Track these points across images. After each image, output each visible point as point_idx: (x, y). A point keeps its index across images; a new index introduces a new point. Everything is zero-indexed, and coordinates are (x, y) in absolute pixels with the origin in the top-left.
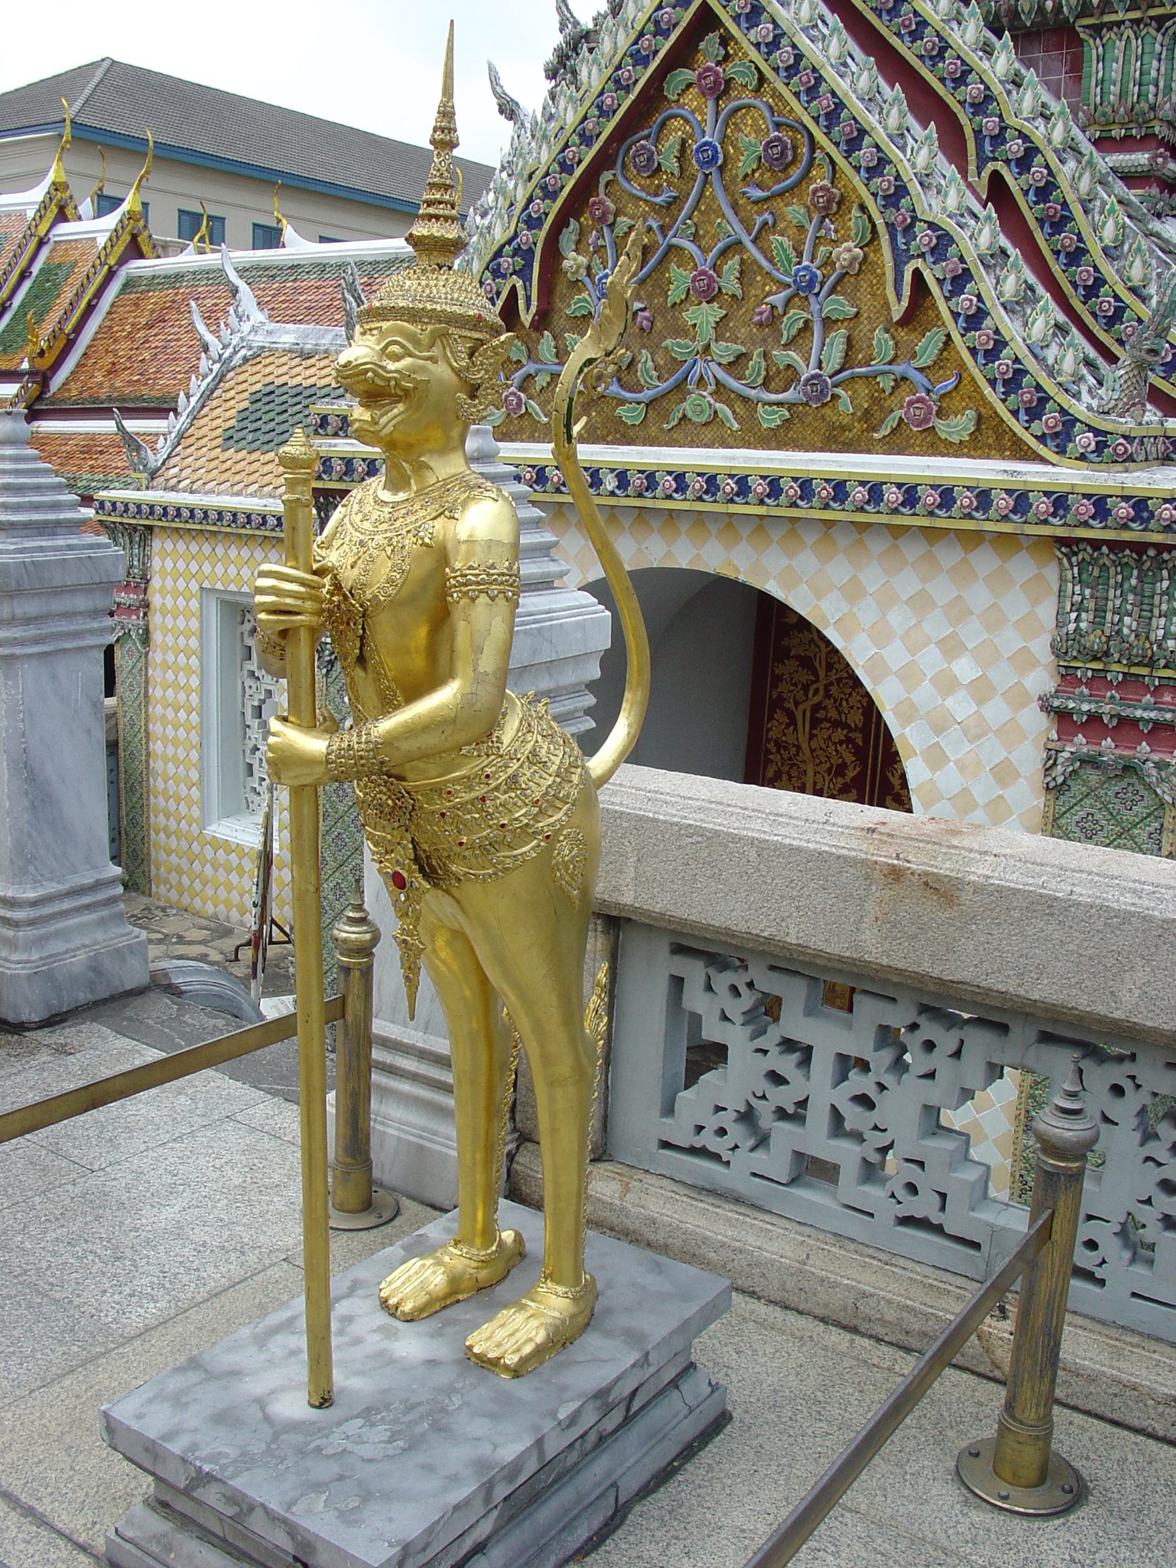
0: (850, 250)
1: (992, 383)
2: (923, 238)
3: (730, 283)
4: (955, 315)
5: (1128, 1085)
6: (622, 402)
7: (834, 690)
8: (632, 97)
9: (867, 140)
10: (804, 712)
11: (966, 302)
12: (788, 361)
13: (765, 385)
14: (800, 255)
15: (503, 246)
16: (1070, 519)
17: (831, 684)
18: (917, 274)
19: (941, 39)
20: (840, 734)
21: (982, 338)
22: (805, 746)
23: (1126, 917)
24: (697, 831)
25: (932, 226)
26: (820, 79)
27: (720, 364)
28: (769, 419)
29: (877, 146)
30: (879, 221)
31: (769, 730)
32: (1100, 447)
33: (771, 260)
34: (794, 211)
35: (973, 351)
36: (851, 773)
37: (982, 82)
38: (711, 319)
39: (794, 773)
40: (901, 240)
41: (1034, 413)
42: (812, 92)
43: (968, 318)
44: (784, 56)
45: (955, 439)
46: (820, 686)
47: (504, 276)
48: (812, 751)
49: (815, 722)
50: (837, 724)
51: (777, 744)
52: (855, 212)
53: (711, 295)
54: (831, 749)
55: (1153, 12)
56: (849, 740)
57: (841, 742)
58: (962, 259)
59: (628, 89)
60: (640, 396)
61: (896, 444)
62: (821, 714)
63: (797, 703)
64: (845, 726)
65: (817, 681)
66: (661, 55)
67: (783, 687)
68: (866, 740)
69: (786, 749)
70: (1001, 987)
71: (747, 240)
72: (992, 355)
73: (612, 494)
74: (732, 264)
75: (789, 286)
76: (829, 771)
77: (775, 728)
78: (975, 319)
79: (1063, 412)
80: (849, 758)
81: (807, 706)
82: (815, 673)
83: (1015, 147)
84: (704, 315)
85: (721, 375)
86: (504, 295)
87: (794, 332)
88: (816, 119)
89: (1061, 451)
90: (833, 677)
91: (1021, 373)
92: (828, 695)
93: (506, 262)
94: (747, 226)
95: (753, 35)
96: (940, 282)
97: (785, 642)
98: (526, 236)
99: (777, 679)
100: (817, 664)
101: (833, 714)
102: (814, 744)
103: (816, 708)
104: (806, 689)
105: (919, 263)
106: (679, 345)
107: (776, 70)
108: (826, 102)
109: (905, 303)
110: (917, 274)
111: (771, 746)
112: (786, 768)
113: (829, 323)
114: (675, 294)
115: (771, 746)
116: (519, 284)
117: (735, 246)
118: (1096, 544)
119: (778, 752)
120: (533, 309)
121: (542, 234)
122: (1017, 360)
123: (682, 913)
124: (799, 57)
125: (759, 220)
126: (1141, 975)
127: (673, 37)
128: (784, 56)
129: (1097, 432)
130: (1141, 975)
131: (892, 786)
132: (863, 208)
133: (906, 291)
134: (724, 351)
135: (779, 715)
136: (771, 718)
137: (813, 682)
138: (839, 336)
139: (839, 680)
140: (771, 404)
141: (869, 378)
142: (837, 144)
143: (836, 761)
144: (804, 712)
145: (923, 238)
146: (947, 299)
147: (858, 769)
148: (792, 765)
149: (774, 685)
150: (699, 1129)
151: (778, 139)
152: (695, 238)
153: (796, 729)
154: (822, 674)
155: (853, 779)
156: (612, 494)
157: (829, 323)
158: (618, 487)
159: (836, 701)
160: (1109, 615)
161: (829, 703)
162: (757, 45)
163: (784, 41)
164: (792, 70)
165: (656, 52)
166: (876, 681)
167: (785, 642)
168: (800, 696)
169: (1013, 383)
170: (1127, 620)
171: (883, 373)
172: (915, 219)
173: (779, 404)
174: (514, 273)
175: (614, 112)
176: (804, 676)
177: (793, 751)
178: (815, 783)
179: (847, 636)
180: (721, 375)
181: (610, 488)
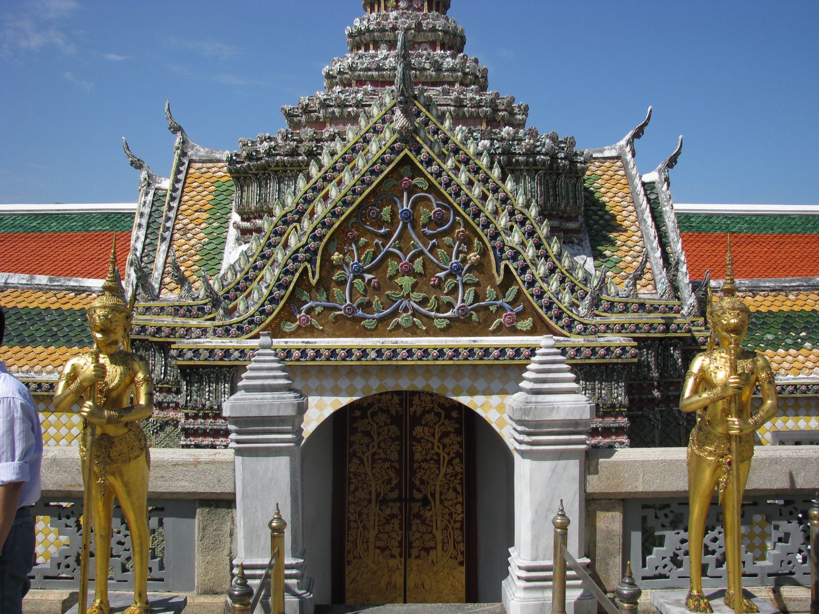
0: (475, 256)
1: (541, 307)
2: (508, 252)
3: (418, 265)
4: (524, 282)
5: (794, 510)
6: (365, 319)
7: (382, 445)
8: (370, 188)
9: (482, 214)
10: (368, 457)
11: (527, 276)
12: (448, 300)
13: (438, 311)
14: (451, 257)
15: (299, 249)
16: (582, 356)
17: (381, 442)
18: (506, 266)
19: (487, 175)
20: (387, 464)
21: (535, 290)
22: (369, 473)
23: (797, 459)
24: (665, 461)
25: (512, 248)
26: (461, 189)
27: (415, 302)
28: (440, 324)
29: (487, 217)
30: (489, 246)
31: (349, 468)
32: (586, 329)
33: (438, 259)
34: (447, 240)
35: (532, 295)
36: (394, 482)
37: (504, 192)
38: (410, 283)
39: (365, 486)
40: (498, 253)
41: (559, 317)
42: (457, 194)
43: (529, 283)
44: (444, 178)
45: (525, 329)
46: (375, 443)
47: (300, 262)
48: (374, 475)
49: (374, 461)
50: (384, 460)
51: (355, 474)
52: (476, 241)
53: (410, 272)
54: (384, 471)
55: (535, 168)
56: (392, 467)
57: (388, 468)
58: (525, 261)
59: (369, 185)
60: (376, 315)
61: (498, 331)
62: (377, 457)
63: (363, 453)
64: (389, 460)
65: (373, 441)
66: (385, 172)
67: (356, 447)
68: (401, 465)
69: (359, 475)
70: (765, 487)
71: (426, 251)
72: (540, 297)
73: (374, 360)
74: (419, 260)
75: (444, 270)
76: (383, 483)
77: (353, 466)
78: (532, 284)
79: (570, 317)
80: (393, 475)
81: (369, 454)
82: (372, 438)
83: (519, 217)
84: (406, 281)
85: (416, 306)
86: (300, 270)
87: (450, 288)
88: (459, 205)
89: (570, 332)
90: (381, 438)
91: (552, 303)
92: (379, 447)
93: (301, 256)
94: (426, 245)
95: (429, 169)
96: (516, 269)
97: (355, 425)
98: (312, 245)
99: (352, 443)
100: (372, 433)
101: (383, 456)
102: (374, 471)
103: (374, 454)
104: (368, 446)
105: (507, 262)
106: (394, 294)
107: (440, 184)
108: (463, 198)
109: (502, 277)
110: (506, 266)
111: (352, 476)
112: (360, 485)
113: (465, 285)
114: (390, 271)
115: (352, 476)
116: (309, 266)
117: (421, 253)
118: (591, 365)
119: (356, 478)
120: (317, 277)
121: (323, 244)
122: (550, 298)
123: (661, 489)
124: (451, 180)
125: (431, 243)
126: (803, 474)
127: (391, 166)
128: (444, 178)
129: (584, 324)
130: (803, 474)
131: (415, 485)
132: (480, 239)
133: (502, 272)
134: (417, 296)
135: (355, 460)
136: (350, 462)
137: (371, 442)
138: (471, 291)
139: (384, 440)
140: (441, 318)
141: (486, 308)
142: (469, 215)
143: (386, 477)
144: (368, 457)
145: (508, 252)
146: (520, 276)
147: (398, 480)
148: (363, 483)
149: (351, 446)
150: (657, 568)
151: (439, 211)
152: (400, 249)
153: (364, 465)
154: (375, 437)
155: (396, 485)
156: (374, 360)
157: (465, 285)
158: (377, 357)
159: (383, 449)
160: (597, 390)
161: (380, 451)
162: (431, 174)
163: (444, 173)
164: (448, 185)
165: (382, 171)
166: (501, 428)
167: (355, 425)
168: (365, 449)
169: (549, 307)
170: (603, 392)
171: (492, 305)
172: (504, 245)
173: (445, 318)
174: (306, 260)
175: (361, 194)
176: (366, 440)
177: (363, 476)
178: (376, 490)
179: (485, 411)
180: (416, 306)
181: (373, 357)
